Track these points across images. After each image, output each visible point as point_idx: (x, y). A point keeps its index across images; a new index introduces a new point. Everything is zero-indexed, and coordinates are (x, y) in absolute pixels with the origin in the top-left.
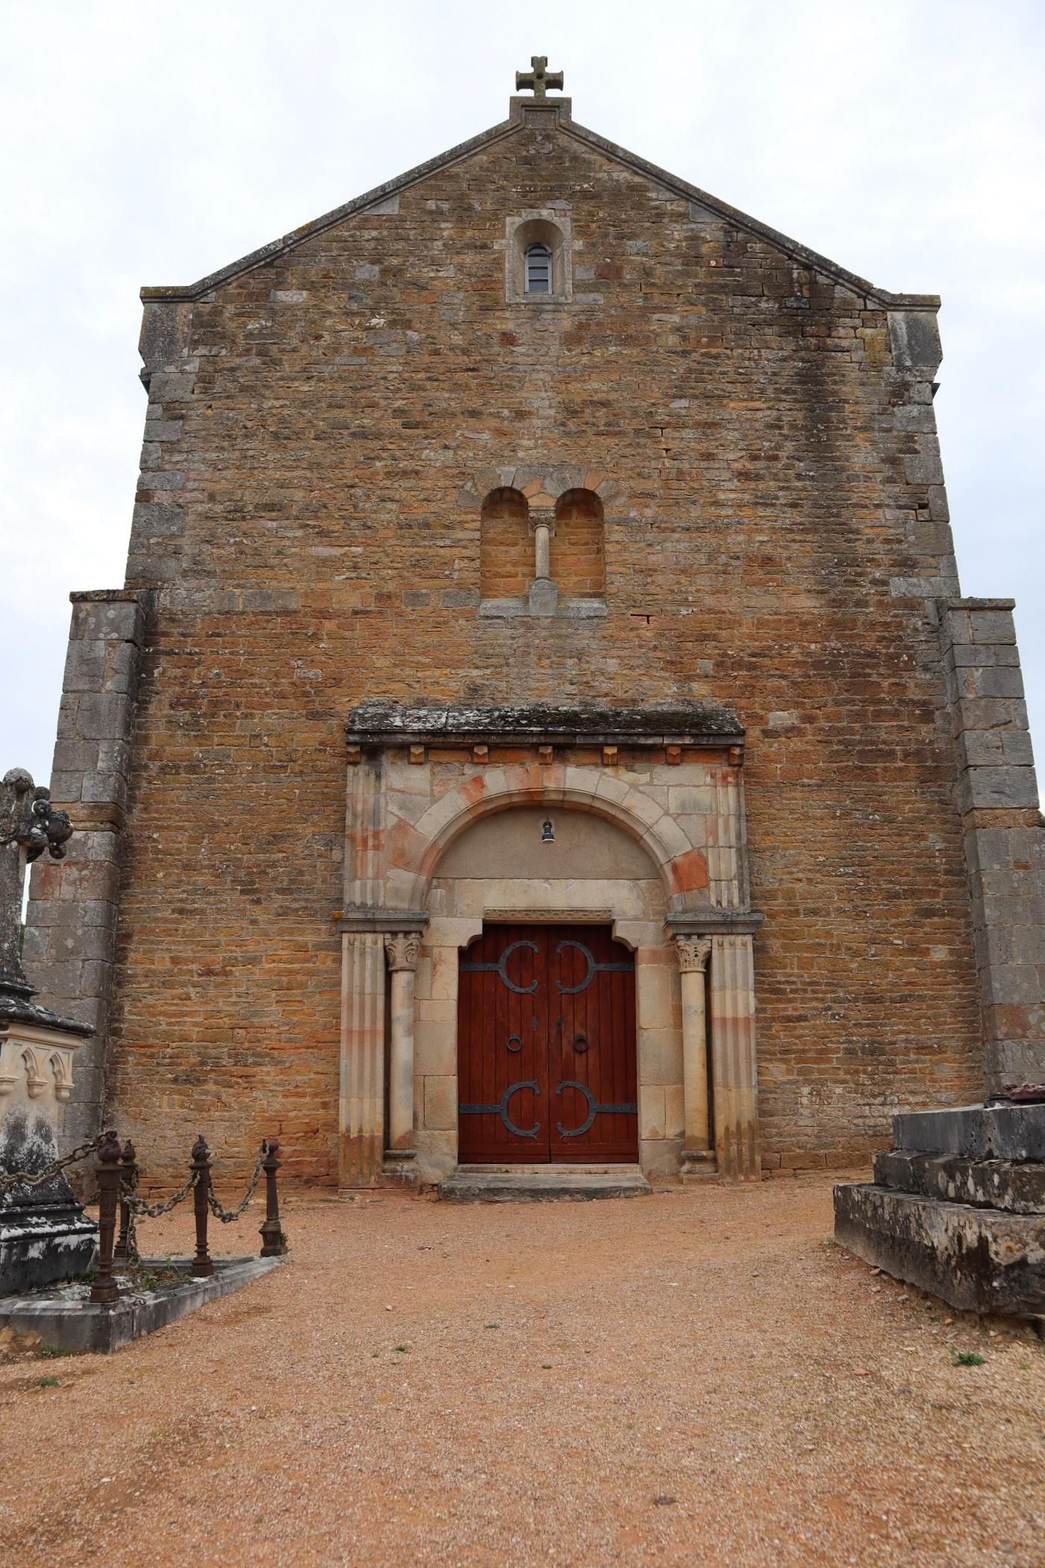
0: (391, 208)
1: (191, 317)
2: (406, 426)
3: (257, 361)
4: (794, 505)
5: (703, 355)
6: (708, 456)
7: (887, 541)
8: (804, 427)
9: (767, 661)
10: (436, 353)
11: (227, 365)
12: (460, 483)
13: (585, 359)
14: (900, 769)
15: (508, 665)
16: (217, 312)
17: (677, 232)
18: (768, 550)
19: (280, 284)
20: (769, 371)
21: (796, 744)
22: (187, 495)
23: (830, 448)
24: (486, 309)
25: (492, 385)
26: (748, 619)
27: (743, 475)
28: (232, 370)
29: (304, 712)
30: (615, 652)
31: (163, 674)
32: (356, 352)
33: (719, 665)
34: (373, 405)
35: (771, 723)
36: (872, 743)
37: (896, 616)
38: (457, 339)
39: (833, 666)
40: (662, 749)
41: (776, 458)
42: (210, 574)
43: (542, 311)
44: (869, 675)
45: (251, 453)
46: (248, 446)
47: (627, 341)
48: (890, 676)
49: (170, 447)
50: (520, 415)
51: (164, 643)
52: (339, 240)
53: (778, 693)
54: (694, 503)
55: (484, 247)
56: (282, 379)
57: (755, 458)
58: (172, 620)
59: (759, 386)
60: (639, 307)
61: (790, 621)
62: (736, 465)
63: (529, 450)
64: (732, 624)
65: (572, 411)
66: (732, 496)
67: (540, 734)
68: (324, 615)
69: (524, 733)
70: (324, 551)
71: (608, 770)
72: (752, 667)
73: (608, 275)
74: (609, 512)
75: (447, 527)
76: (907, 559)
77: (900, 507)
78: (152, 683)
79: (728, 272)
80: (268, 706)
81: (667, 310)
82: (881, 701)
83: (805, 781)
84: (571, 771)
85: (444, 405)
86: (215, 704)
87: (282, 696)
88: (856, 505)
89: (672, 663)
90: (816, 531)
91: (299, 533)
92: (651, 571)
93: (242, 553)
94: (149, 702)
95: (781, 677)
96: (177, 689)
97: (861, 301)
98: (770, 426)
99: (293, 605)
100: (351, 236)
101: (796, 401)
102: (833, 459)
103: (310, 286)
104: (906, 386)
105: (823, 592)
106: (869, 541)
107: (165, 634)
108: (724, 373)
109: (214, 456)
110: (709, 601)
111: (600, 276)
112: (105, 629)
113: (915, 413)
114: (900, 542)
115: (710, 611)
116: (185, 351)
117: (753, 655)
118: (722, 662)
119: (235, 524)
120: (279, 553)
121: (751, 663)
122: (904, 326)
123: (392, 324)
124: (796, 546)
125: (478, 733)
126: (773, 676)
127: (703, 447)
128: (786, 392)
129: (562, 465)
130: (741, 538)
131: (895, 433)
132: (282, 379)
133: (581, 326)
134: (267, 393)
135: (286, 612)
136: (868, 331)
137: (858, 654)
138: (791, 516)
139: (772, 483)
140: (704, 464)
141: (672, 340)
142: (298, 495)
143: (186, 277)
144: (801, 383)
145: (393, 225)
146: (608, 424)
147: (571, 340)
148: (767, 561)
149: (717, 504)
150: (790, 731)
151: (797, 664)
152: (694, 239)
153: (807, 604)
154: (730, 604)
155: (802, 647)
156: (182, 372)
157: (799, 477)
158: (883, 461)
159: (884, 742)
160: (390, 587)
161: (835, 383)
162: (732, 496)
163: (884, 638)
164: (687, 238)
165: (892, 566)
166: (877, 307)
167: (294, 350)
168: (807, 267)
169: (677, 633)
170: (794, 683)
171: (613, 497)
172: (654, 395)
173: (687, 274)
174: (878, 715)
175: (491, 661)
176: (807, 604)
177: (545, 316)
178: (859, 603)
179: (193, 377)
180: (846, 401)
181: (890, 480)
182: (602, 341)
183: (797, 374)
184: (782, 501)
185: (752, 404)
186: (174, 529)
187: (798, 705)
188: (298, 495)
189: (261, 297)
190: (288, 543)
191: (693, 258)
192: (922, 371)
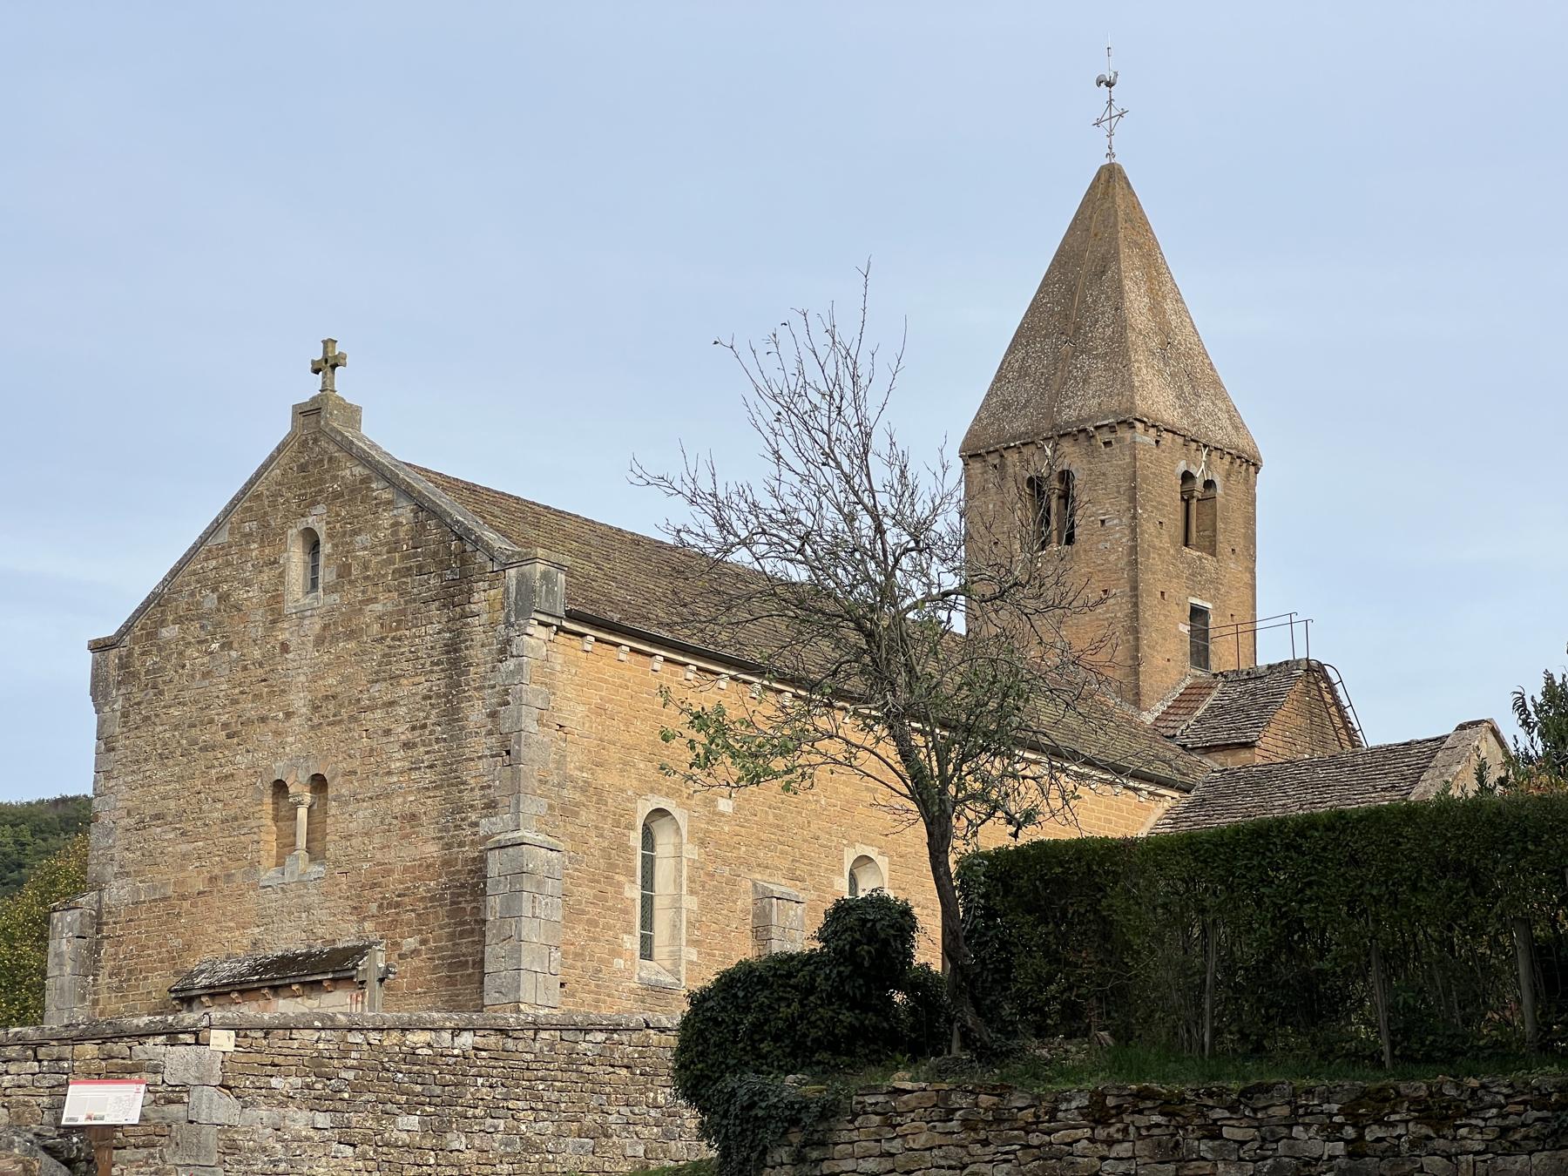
0: (224, 537)
1: (117, 661)
2: (229, 736)
3: (151, 692)
4: (431, 767)
5: (393, 639)
6: (387, 732)
7: (482, 788)
8: (445, 695)
9: (406, 899)
10: (245, 668)
11: (137, 700)
12: (254, 780)
13: (326, 657)
14: (469, 975)
15: (273, 922)
16: (130, 654)
17: (386, 519)
18: (414, 809)
19: (162, 623)
20: (429, 645)
21: (416, 962)
22: (117, 813)
23: (456, 710)
24: (274, 622)
25: (274, 692)
26: (399, 867)
27: (407, 745)
28: (139, 704)
29: (172, 971)
30: (327, 904)
31: (105, 954)
32: (205, 675)
33: (380, 906)
34: (211, 722)
35: (404, 949)
36: (457, 956)
37: (480, 851)
38: (257, 654)
39: (442, 898)
40: (320, 982)
41: (424, 726)
42: (128, 874)
43: (304, 618)
44: (460, 903)
45: (148, 773)
46: (147, 768)
47: (351, 635)
48: (472, 901)
49: (108, 775)
50: (288, 715)
51: (106, 931)
52: (195, 573)
53: (409, 924)
54: (377, 774)
55: (275, 562)
56: (164, 707)
57: (413, 728)
58: (109, 912)
59: (422, 661)
60: (360, 602)
61: (420, 865)
62: (403, 737)
63: (293, 744)
64: (389, 872)
65: (316, 708)
66: (398, 764)
67: (258, 980)
68: (183, 897)
69: (248, 982)
70: (185, 847)
71: (299, 999)
72: (398, 905)
73: (344, 571)
74: (331, 792)
75: (246, 818)
76: (493, 801)
77: (492, 756)
78: (100, 961)
79: (413, 554)
80: (156, 969)
81: (374, 600)
82: (464, 923)
83: (419, 990)
84: (281, 1002)
85: (248, 715)
86: (130, 972)
87: (162, 961)
88: (466, 760)
89: (355, 908)
90: (441, 786)
91: (172, 836)
92: (348, 837)
93: (143, 855)
94: (98, 975)
95: (412, 911)
96: (112, 963)
97: (490, 564)
98: (426, 698)
99: (170, 892)
100: (202, 568)
101: (442, 670)
102: (457, 720)
103: (179, 620)
104: (508, 641)
105: (441, 838)
106: (472, 790)
107: (106, 924)
108: (402, 654)
109: (129, 779)
110: (379, 855)
111: (339, 576)
112: (66, 931)
113: (512, 668)
114: (489, 787)
115: (379, 864)
116: (114, 692)
117: (399, 896)
118: (382, 904)
119: (140, 832)
120: (162, 853)
121: (396, 902)
122: (514, 582)
123: (222, 646)
124: (429, 801)
125: (234, 984)
126: (407, 911)
127: (385, 725)
128: (437, 664)
129: (306, 758)
130: (400, 800)
131: (497, 689)
132: (164, 707)
133: (325, 627)
134: (157, 720)
135: (165, 899)
136: (492, 592)
137: (456, 886)
138: (430, 775)
139: (422, 749)
140: (385, 740)
141: (376, 627)
142: (172, 804)
143: (109, 630)
144: (448, 652)
145: (225, 551)
146: (334, 716)
147: (319, 641)
148: (413, 816)
149: (389, 773)
150: (416, 952)
151: (422, 899)
152: (396, 524)
153: (432, 850)
154: (390, 856)
155: (426, 885)
156: (113, 710)
157: (437, 741)
158: (489, 716)
159: (463, 955)
160: (216, 871)
161: (467, 648)
162: (398, 764)
163: (472, 870)
164: (393, 525)
165: (483, 809)
166: (500, 568)
167: (171, 681)
168: (460, 539)
169: (360, 884)
170: (419, 915)
171: (333, 778)
172: (362, 683)
173: (390, 562)
174: (462, 934)
175: (265, 921)
176: (432, 850)
177: (307, 622)
178: (461, 844)
179: (119, 714)
180: (470, 665)
181: (490, 733)
182: (335, 639)
183: (445, 645)
184: (426, 764)
185: (417, 680)
186: (110, 841)
187: (420, 932)
188: (172, 804)
189: (152, 635)
190: (166, 844)
191: (394, 547)
192: (519, 625)
